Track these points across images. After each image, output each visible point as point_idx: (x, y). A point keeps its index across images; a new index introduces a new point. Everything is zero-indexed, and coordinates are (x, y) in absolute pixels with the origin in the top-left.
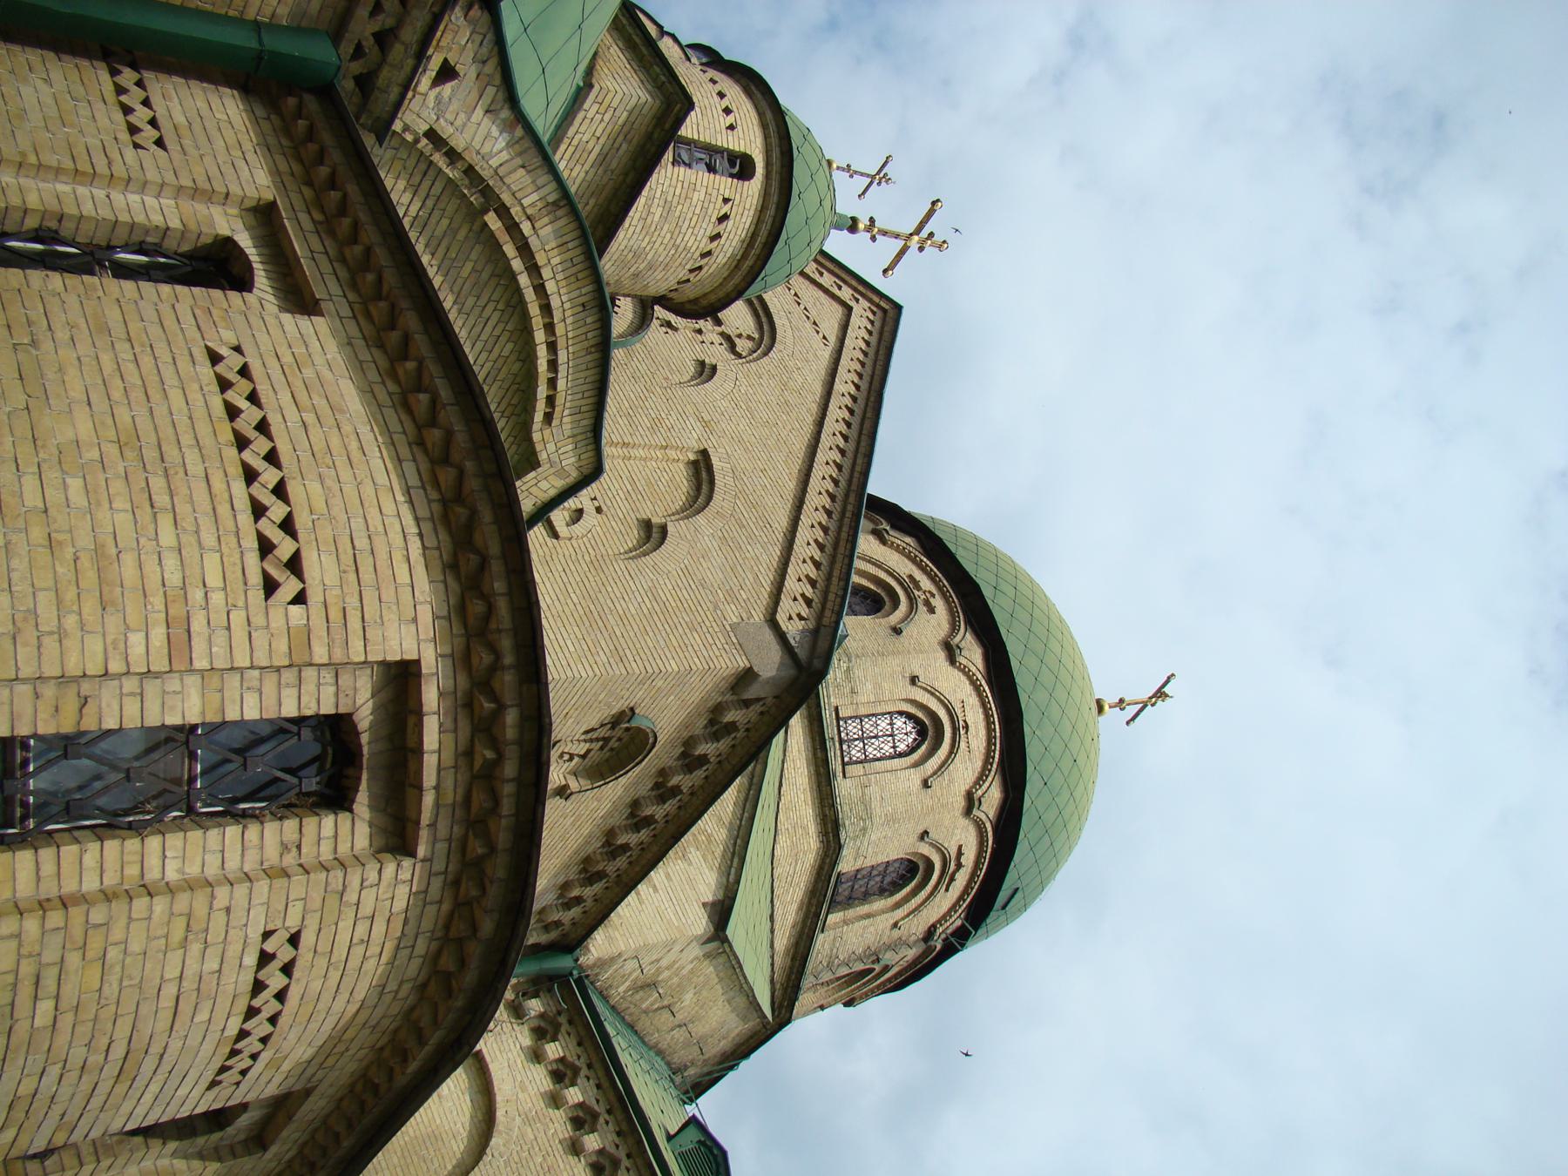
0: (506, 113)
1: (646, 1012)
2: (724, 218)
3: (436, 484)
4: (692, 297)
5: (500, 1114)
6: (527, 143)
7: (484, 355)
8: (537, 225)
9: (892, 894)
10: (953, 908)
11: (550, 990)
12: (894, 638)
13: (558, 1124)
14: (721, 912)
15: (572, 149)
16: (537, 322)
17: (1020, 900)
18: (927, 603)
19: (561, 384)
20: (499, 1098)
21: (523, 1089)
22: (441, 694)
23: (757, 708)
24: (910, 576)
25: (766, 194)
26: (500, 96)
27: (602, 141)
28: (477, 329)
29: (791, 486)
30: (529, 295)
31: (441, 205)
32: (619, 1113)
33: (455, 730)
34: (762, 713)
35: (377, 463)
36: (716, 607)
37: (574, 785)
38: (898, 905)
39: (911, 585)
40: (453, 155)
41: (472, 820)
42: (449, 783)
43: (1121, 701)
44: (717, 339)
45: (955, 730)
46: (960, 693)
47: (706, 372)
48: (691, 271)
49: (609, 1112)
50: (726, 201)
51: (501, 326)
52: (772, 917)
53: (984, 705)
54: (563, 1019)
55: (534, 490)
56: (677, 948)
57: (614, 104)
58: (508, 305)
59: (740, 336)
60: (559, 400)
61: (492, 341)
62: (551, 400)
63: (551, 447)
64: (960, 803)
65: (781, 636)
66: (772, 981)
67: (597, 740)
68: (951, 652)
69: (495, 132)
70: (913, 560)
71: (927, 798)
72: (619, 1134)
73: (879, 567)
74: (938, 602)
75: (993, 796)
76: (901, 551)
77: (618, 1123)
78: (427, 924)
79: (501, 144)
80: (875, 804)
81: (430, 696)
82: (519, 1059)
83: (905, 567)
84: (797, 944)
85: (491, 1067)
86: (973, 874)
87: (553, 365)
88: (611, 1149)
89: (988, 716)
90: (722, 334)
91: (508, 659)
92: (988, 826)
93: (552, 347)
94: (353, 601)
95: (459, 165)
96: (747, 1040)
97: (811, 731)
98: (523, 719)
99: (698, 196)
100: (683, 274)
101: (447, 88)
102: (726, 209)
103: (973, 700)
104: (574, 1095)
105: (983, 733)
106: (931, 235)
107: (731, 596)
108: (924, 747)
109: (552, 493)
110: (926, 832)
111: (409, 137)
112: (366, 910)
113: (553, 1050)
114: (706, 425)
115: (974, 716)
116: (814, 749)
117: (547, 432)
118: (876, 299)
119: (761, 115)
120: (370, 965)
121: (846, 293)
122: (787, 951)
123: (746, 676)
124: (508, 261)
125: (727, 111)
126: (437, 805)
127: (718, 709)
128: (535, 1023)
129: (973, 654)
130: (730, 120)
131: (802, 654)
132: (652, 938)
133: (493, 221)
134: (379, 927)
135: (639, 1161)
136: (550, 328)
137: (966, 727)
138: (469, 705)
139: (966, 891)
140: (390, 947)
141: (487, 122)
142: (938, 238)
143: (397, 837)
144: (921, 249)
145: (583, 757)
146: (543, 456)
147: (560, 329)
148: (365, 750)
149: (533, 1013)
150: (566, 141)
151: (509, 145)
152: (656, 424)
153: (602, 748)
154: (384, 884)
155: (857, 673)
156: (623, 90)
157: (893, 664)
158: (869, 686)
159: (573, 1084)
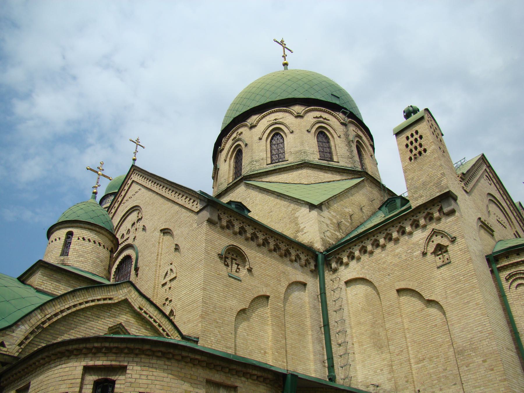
0: (14, 328)
1: (351, 224)
2: (84, 239)
3: (55, 360)
4: (110, 242)
5: (361, 276)
6: (23, 320)
7: (90, 319)
8: (47, 313)
9: (329, 139)
10: (335, 117)
11: (330, 260)
12: (248, 146)
13: (365, 258)
14: (312, 206)
15: (55, 290)
16: (78, 308)
17: (337, 92)
18: (240, 134)
19: (99, 297)
20: (357, 276)
21: (355, 269)
22: (91, 360)
23: (221, 216)
24: (233, 140)
25: (77, 227)
26: (9, 330)
27: (52, 282)
28: (82, 322)
29: (170, 204)
30: (70, 311)
31: (43, 338)
32: (363, 239)
33: (99, 357)
34: (224, 213)
35: (50, 373)
36: (193, 230)
37: (247, 267)
38: (333, 136)
39: (235, 140)
40: (26, 338)
41: (119, 352)
42: (111, 358)
43: (283, 56)
44: (138, 223)
45: (276, 123)
46: (264, 122)
47: (144, 229)
48: (100, 245)
49: (362, 242)
50: (79, 239)
51: (81, 316)
53: (269, 114)
54: (337, 256)
55: (135, 299)
56: (323, 219)
57: (41, 281)
58: (74, 315)
59: (138, 217)
60: (105, 297)
61: (86, 318)
63: (120, 296)
64: (299, 120)
65: (201, 210)
66: (351, 179)
67: (232, 262)
68: (252, 127)
69: (19, 329)
70: (228, 139)
72: (368, 239)
74: (240, 131)
75: (298, 109)
76: (226, 143)
77: (365, 240)
78: (147, 361)
79: (23, 327)
80: (297, 149)
81: (91, 363)
82: (348, 270)
83: (230, 142)
84: (339, 172)
85: (349, 279)
86: (324, 111)
87: (93, 301)
88: (372, 241)
89: (273, 112)
90: (137, 222)
91: (84, 345)
92: (307, 109)
93: (87, 302)
94: (70, 381)
95: (29, 336)
96: (374, 183)
97: (271, 174)
98: (97, 342)
99: (77, 247)
100: (101, 248)
101: (6, 343)
102: (81, 239)
103: (268, 118)
104: (357, 253)
106: (98, 168)
107: (191, 225)
108: (282, 133)
109: (136, 293)
110: (307, 131)
111: (21, 350)
112: (138, 376)
113: (345, 260)
114: (155, 230)
115: (272, 117)
117: (115, 298)
118: (131, 172)
119: (57, 230)
120: (155, 374)
121: (130, 182)
122: (341, 175)
123: (210, 221)
124: (58, 319)
125: (56, 240)
126: (115, 361)
127: (222, 227)
128: (339, 264)
129: (254, 119)
130: (58, 239)
131: (205, 204)
132: (317, 229)
133: (47, 325)
134: (145, 373)
135: (375, 233)
136: (81, 304)
137: (276, 119)
138: (95, 354)
139: (330, 113)
140: (151, 369)
141: (16, 332)
142: (99, 165)
143: (122, 369)
144: (103, 170)
145: (238, 265)
146: (123, 298)
147: (81, 301)
148: (103, 377)
149: (336, 266)
150: (53, 292)
151: (23, 325)
152: (154, 246)
153: (235, 260)
154: (132, 373)
155: (257, 158)
156: (38, 279)
157: (255, 146)
158: (261, 154)
159: (354, 253)
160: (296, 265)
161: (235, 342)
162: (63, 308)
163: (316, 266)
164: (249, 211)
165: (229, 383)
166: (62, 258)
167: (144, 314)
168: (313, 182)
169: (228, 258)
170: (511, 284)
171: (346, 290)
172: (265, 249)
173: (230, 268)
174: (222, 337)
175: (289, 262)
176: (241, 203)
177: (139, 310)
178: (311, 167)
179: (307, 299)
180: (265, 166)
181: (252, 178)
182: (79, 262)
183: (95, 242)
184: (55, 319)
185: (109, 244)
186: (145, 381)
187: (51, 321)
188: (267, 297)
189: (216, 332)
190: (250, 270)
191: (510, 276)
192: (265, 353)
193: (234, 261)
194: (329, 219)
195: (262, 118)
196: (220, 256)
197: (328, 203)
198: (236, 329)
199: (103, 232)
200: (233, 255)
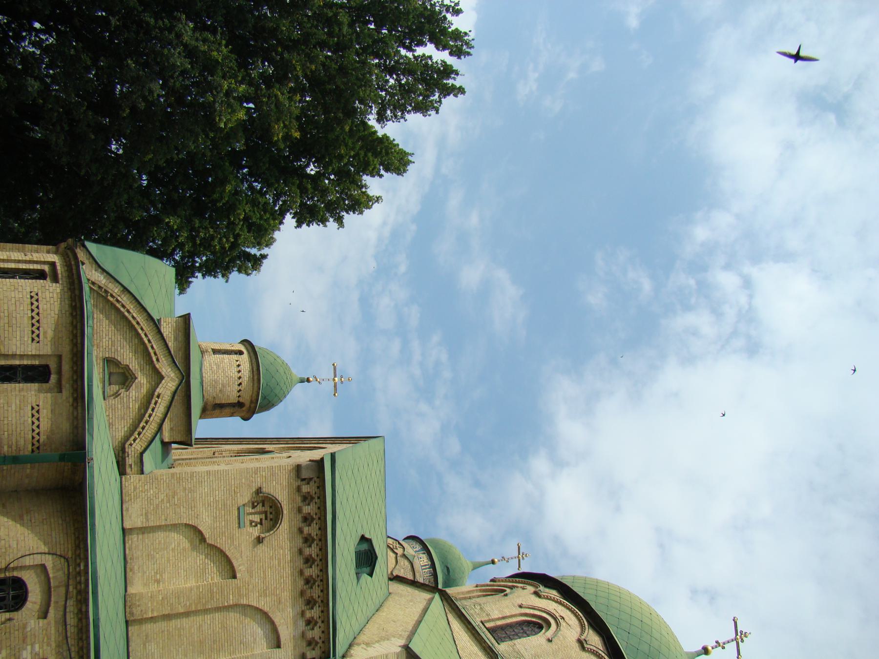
19: (155, 346)
23: (312, 483)
25: (250, 357)
45: (555, 619)
53: (568, 608)
62: (155, 354)
64: (576, 646)
71: (553, 645)
78: (66, 296)
97: (462, 621)
100: (237, 388)
105: (569, 613)
106: (342, 377)
109: (174, 388)
127: (299, 489)
133: (111, 299)
134: (55, 295)
146: (163, 374)
153: (266, 519)
160: (301, 624)
161: (159, 528)
162: (131, 311)
164: (371, 575)
165: (64, 383)
166: (210, 350)
167: (153, 401)
169: (263, 506)
172: (300, 563)
173: (251, 510)
174: (157, 506)
175: (299, 610)
176: (376, 558)
177: (156, 394)
179: (257, 651)
180: (478, 620)
181: (447, 601)
182: (210, 365)
183: (240, 378)
184: (118, 305)
185: (246, 398)
186: (48, 295)
187: (115, 303)
188: (234, 577)
189: (162, 496)
190: (259, 540)
192: (158, 582)
193: (263, 516)
195: (557, 602)
196: (259, 491)
198: (174, 527)
199: (256, 385)
200: (271, 513)
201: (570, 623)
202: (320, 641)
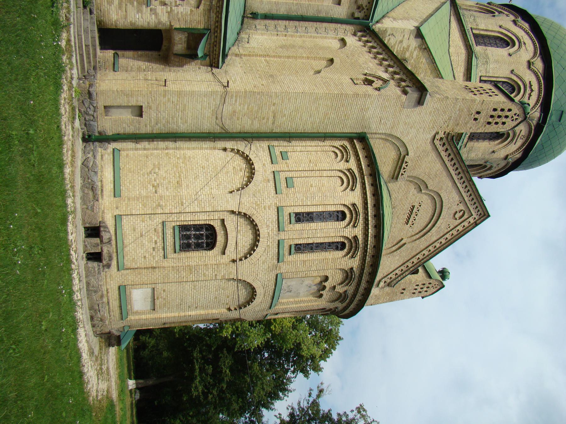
45: (520, 42)
52: (454, 76)
56: (406, 36)
64: (525, 64)
73: (519, 78)
97: (459, 24)
116: (461, 28)
137: (525, 44)
163: (358, 18)
168: (452, 58)
170: (337, 148)
171: (335, 38)
178: (468, 58)
179: (325, 4)
180: (470, 26)
181: (454, 8)
191: (345, 148)
194: (409, 46)
197: (425, 49)
201: (528, 48)
202: (366, 8)
